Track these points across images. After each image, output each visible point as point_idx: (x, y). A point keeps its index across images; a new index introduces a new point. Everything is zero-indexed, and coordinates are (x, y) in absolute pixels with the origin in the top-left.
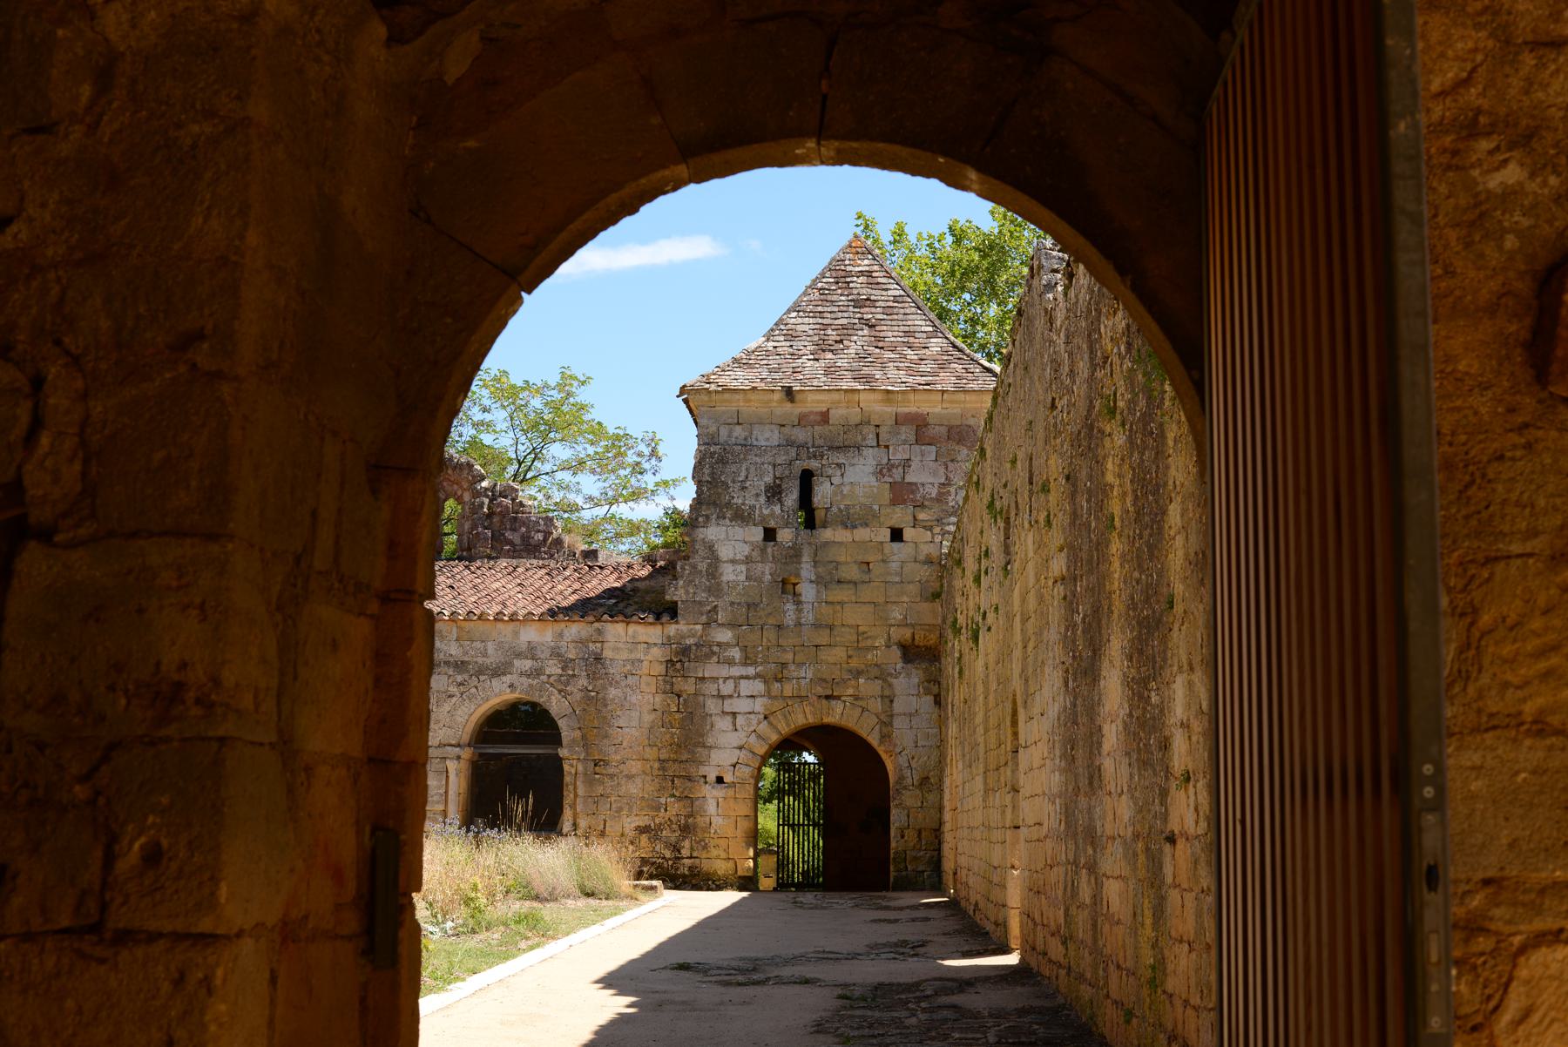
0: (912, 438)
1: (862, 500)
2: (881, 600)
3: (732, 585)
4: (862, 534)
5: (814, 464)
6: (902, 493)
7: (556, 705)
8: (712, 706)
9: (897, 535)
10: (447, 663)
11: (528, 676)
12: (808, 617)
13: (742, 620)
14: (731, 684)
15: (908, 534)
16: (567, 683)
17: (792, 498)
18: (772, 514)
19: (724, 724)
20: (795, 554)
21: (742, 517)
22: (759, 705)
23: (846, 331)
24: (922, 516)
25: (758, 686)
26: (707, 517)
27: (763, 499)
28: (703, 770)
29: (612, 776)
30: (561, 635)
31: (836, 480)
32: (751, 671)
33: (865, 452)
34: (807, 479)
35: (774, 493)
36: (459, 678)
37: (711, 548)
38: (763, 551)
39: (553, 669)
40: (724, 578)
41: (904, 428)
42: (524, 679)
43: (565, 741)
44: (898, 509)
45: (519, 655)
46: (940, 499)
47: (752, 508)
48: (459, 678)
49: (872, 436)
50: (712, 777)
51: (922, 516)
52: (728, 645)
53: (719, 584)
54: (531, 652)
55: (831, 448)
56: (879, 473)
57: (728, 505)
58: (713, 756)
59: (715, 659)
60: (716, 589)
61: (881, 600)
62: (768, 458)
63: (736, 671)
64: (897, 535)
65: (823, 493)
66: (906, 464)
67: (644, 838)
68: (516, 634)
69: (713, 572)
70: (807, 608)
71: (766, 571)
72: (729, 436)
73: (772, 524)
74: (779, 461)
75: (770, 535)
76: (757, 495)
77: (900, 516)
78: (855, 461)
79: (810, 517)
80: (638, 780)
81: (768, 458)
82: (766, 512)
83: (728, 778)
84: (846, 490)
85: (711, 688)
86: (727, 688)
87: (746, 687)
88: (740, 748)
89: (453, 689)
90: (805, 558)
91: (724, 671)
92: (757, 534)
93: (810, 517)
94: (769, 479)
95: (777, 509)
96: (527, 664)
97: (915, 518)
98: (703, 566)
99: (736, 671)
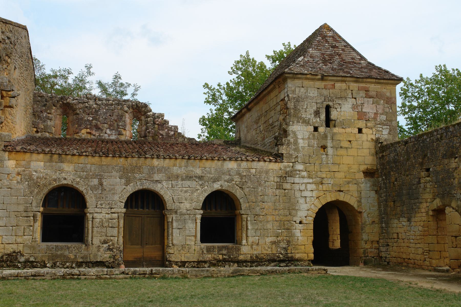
0: (364, 95)
1: (348, 118)
2: (356, 155)
3: (303, 148)
4: (348, 130)
5: (331, 104)
6: (361, 116)
7: (239, 193)
8: (298, 194)
9: (360, 131)
10: (196, 177)
11: (228, 182)
12: (331, 160)
13: (307, 161)
14: (304, 185)
15: (364, 130)
16: (243, 185)
17: (323, 116)
18: (317, 121)
19: (302, 201)
20: (325, 136)
21: (306, 122)
22: (315, 194)
23: (331, 56)
24: (369, 124)
25: (313, 187)
26: (293, 122)
27: (313, 116)
28: (295, 219)
29: (261, 222)
30: (240, 165)
31: (339, 110)
32: (311, 181)
33: (349, 100)
34: (328, 108)
35: (317, 113)
36: (200, 182)
37: (294, 133)
38: (314, 135)
39: (237, 179)
40: (300, 145)
41: (361, 92)
42: (226, 183)
43: (242, 208)
44: (360, 121)
45: (223, 174)
46: (375, 119)
47: (309, 119)
48: (200, 182)
49: (350, 94)
50: (298, 222)
51: (369, 124)
52: (302, 171)
53: (298, 148)
54: (229, 172)
55: (336, 98)
56: (354, 107)
57: (301, 118)
58: (298, 213)
59: (298, 176)
60: (297, 150)
61: (356, 155)
62: (314, 101)
63: (306, 180)
64: (360, 131)
65: (334, 114)
66: (362, 104)
67: (274, 246)
68: (222, 165)
69: (296, 143)
70: (330, 157)
71: (315, 143)
72: (299, 92)
73: (317, 125)
74: (318, 102)
75: (316, 129)
76: (311, 114)
77: (361, 124)
78: (345, 103)
79: (328, 122)
80: (271, 223)
81: (314, 101)
82: (314, 121)
83: (304, 221)
84: (342, 114)
85: (297, 187)
86: (303, 187)
87: (310, 187)
88: (308, 210)
89: (198, 187)
90: (329, 138)
91: (301, 181)
92: (312, 128)
93: (328, 122)
94: (315, 108)
95: (318, 119)
96: (227, 177)
97: (366, 125)
98: (292, 140)
99: (306, 180)
